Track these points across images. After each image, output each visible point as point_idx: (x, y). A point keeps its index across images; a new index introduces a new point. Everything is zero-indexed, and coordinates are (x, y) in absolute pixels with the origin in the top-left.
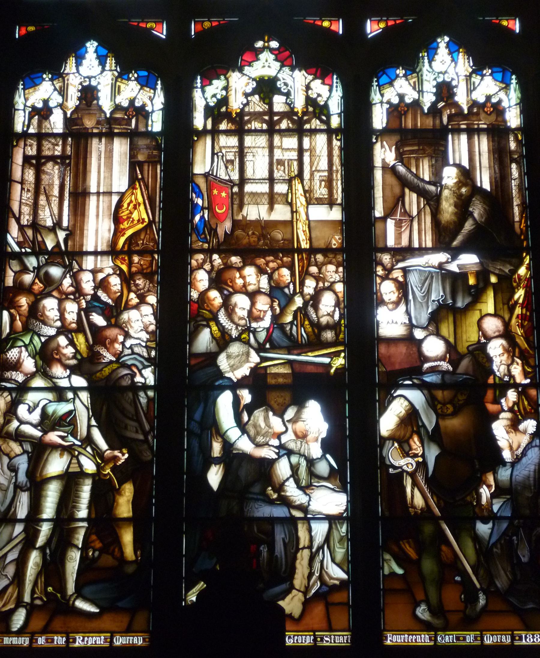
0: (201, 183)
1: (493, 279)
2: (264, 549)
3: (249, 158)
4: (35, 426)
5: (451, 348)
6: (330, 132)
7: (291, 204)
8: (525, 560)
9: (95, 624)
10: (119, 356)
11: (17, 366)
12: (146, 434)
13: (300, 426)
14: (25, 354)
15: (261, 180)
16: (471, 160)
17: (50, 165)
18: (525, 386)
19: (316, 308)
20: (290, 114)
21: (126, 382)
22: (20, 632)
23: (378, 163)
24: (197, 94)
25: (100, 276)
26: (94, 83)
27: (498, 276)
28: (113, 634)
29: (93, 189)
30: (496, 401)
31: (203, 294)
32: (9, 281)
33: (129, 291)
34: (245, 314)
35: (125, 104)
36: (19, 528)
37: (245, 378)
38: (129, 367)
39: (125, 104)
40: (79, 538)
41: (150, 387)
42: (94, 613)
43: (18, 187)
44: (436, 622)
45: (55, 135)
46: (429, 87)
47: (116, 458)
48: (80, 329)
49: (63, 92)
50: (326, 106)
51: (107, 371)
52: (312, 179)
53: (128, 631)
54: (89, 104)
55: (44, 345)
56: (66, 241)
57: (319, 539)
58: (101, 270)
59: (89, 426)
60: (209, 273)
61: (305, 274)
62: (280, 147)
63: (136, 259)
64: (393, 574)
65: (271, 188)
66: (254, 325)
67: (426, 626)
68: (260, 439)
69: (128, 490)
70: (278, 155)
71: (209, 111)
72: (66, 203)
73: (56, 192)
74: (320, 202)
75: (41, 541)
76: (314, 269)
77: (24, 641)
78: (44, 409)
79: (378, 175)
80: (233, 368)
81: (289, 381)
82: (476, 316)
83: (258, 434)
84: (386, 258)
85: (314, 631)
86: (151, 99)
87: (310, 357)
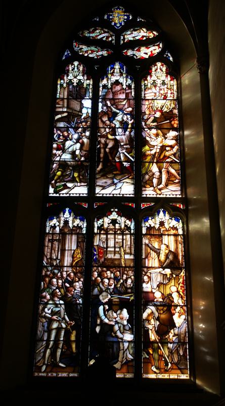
0: (96, 247)
1: (174, 276)
2: (111, 350)
3: (109, 241)
4: (49, 314)
5: (163, 294)
6: (131, 234)
7: (120, 254)
8: (181, 354)
9: (64, 370)
10: (72, 295)
11: (45, 297)
12: (79, 317)
13: (121, 315)
14: (47, 294)
15: (112, 247)
16: (168, 243)
17: (55, 242)
18: (182, 306)
19: (126, 283)
20: (120, 229)
21: (74, 303)
22: (44, 372)
23: (144, 243)
24: (95, 223)
25: (68, 273)
26: (68, 219)
27: (176, 275)
28: (69, 373)
29: (67, 249)
30: (175, 310)
31: (96, 278)
32: (44, 274)
33: (76, 277)
34: (107, 284)
35: (76, 225)
36: (44, 343)
37: (106, 302)
38: (75, 298)
39: (76, 225)
40: (61, 346)
41: (81, 304)
42: (63, 367)
43: (47, 248)
44: (157, 371)
45: (57, 234)
46: (158, 222)
47: (71, 324)
48: (62, 287)
49: (59, 222)
50: (130, 227)
51: (69, 299)
52: (126, 247)
53: (73, 372)
54: (66, 225)
55: (53, 292)
56: (59, 263)
57: (126, 347)
58: (68, 271)
59: (64, 315)
60: (97, 272)
61: (123, 273)
62: (117, 238)
63: (78, 268)
64: (146, 358)
65: (115, 249)
66: (109, 287)
67: (155, 373)
68: (110, 319)
69: (74, 333)
70: (117, 240)
71: (98, 228)
72: (59, 252)
73: (57, 249)
74: (128, 254)
75: (50, 346)
76: (126, 272)
77: (44, 375)
78: (52, 309)
79: (144, 246)
80: (103, 299)
81: (118, 303)
82: (169, 286)
83: (110, 317)
84: (145, 270)
85: (124, 373)
86: (83, 224)
87: (124, 297)
